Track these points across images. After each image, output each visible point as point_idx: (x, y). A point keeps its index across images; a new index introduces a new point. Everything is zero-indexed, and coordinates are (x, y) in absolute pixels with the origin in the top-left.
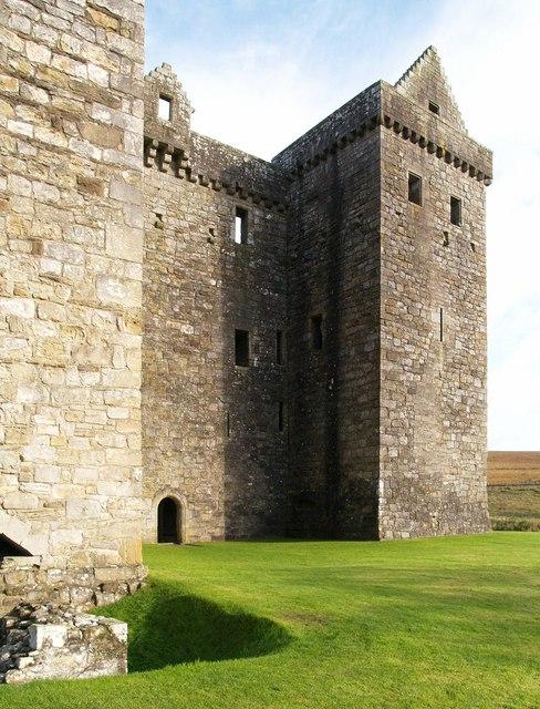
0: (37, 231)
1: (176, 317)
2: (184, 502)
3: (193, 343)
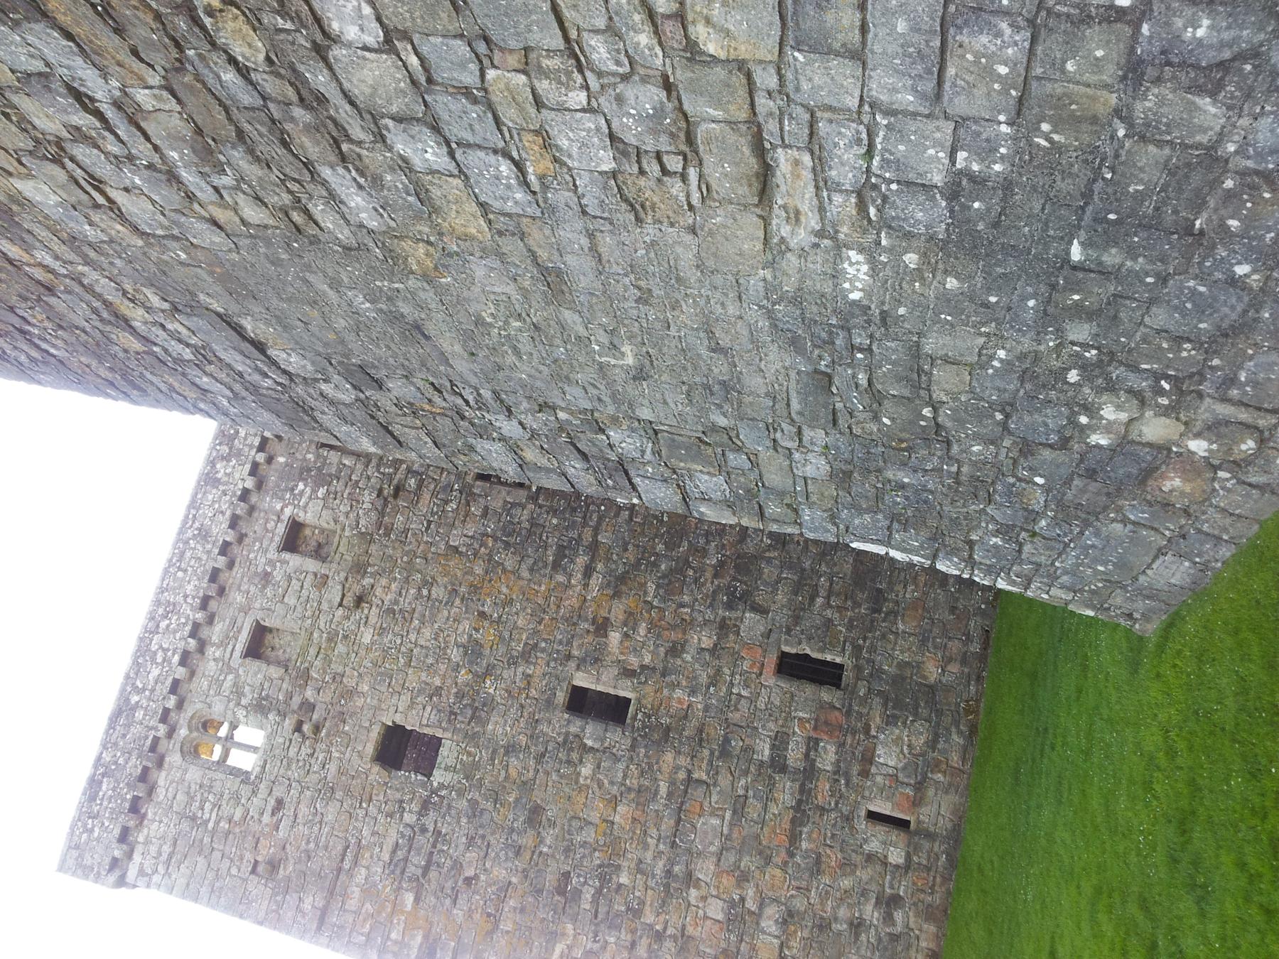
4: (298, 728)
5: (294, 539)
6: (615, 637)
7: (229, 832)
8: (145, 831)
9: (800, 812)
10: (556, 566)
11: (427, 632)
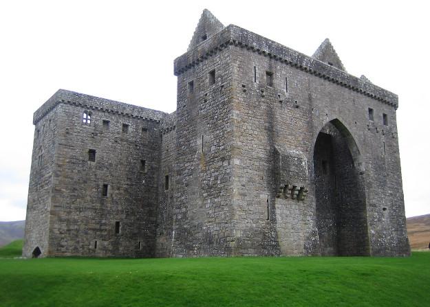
5: (125, 126)
6: (117, 192)
9: (94, 230)
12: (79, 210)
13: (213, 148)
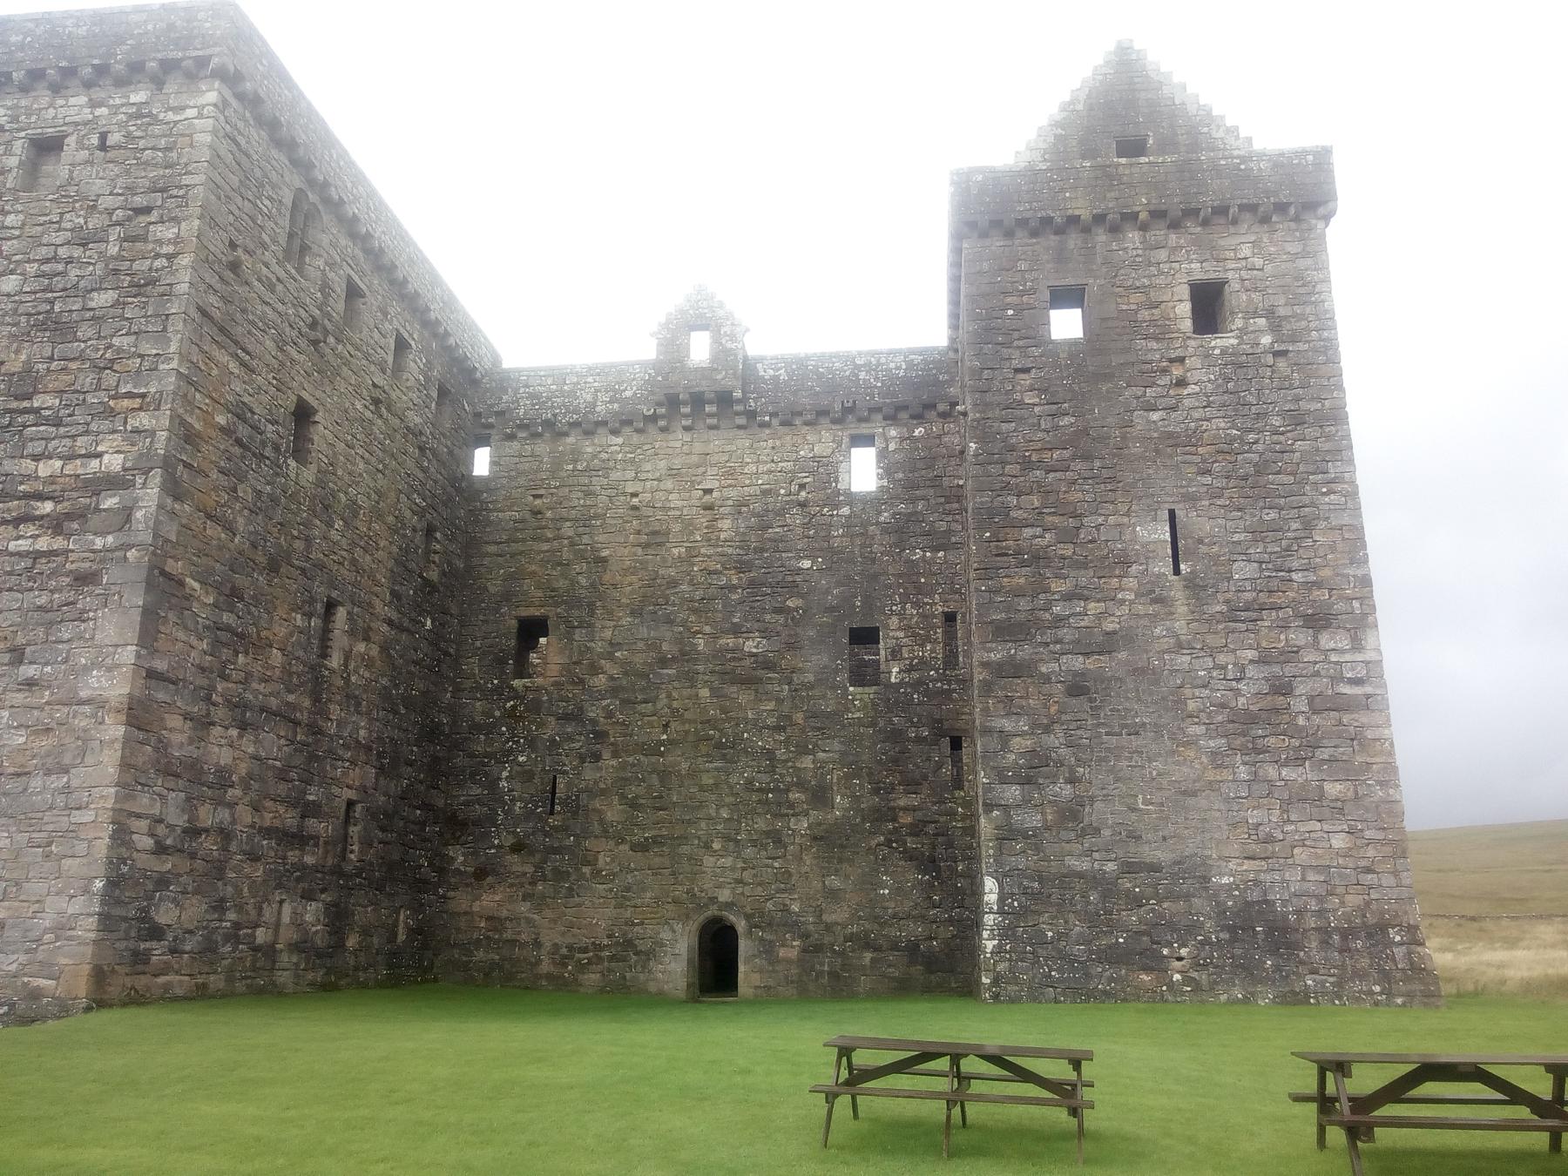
0: (20, 639)
1: (736, 631)
2: (741, 926)
3: (769, 666)
4: (314, 325)
6: (361, 647)
7: (255, 222)
8: (252, 122)
10: (394, 593)
11: (361, 465)
12: (244, 718)
13: (1243, 571)
